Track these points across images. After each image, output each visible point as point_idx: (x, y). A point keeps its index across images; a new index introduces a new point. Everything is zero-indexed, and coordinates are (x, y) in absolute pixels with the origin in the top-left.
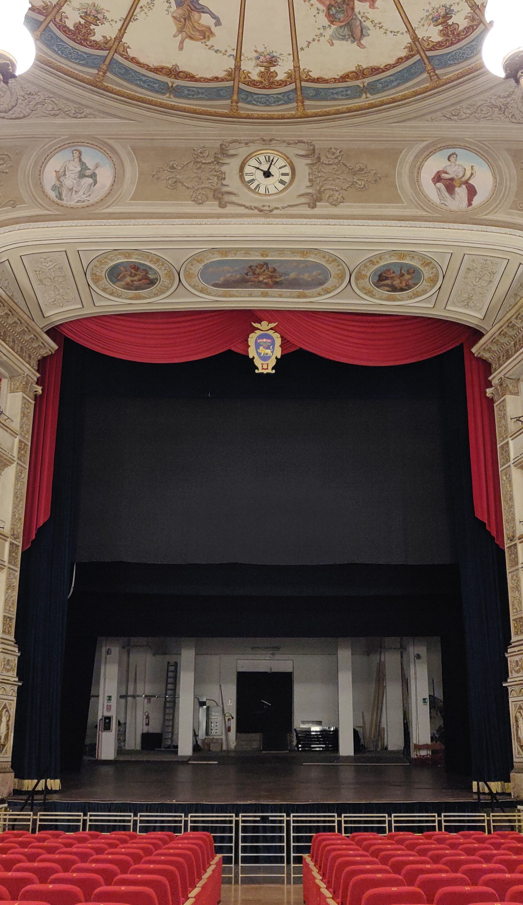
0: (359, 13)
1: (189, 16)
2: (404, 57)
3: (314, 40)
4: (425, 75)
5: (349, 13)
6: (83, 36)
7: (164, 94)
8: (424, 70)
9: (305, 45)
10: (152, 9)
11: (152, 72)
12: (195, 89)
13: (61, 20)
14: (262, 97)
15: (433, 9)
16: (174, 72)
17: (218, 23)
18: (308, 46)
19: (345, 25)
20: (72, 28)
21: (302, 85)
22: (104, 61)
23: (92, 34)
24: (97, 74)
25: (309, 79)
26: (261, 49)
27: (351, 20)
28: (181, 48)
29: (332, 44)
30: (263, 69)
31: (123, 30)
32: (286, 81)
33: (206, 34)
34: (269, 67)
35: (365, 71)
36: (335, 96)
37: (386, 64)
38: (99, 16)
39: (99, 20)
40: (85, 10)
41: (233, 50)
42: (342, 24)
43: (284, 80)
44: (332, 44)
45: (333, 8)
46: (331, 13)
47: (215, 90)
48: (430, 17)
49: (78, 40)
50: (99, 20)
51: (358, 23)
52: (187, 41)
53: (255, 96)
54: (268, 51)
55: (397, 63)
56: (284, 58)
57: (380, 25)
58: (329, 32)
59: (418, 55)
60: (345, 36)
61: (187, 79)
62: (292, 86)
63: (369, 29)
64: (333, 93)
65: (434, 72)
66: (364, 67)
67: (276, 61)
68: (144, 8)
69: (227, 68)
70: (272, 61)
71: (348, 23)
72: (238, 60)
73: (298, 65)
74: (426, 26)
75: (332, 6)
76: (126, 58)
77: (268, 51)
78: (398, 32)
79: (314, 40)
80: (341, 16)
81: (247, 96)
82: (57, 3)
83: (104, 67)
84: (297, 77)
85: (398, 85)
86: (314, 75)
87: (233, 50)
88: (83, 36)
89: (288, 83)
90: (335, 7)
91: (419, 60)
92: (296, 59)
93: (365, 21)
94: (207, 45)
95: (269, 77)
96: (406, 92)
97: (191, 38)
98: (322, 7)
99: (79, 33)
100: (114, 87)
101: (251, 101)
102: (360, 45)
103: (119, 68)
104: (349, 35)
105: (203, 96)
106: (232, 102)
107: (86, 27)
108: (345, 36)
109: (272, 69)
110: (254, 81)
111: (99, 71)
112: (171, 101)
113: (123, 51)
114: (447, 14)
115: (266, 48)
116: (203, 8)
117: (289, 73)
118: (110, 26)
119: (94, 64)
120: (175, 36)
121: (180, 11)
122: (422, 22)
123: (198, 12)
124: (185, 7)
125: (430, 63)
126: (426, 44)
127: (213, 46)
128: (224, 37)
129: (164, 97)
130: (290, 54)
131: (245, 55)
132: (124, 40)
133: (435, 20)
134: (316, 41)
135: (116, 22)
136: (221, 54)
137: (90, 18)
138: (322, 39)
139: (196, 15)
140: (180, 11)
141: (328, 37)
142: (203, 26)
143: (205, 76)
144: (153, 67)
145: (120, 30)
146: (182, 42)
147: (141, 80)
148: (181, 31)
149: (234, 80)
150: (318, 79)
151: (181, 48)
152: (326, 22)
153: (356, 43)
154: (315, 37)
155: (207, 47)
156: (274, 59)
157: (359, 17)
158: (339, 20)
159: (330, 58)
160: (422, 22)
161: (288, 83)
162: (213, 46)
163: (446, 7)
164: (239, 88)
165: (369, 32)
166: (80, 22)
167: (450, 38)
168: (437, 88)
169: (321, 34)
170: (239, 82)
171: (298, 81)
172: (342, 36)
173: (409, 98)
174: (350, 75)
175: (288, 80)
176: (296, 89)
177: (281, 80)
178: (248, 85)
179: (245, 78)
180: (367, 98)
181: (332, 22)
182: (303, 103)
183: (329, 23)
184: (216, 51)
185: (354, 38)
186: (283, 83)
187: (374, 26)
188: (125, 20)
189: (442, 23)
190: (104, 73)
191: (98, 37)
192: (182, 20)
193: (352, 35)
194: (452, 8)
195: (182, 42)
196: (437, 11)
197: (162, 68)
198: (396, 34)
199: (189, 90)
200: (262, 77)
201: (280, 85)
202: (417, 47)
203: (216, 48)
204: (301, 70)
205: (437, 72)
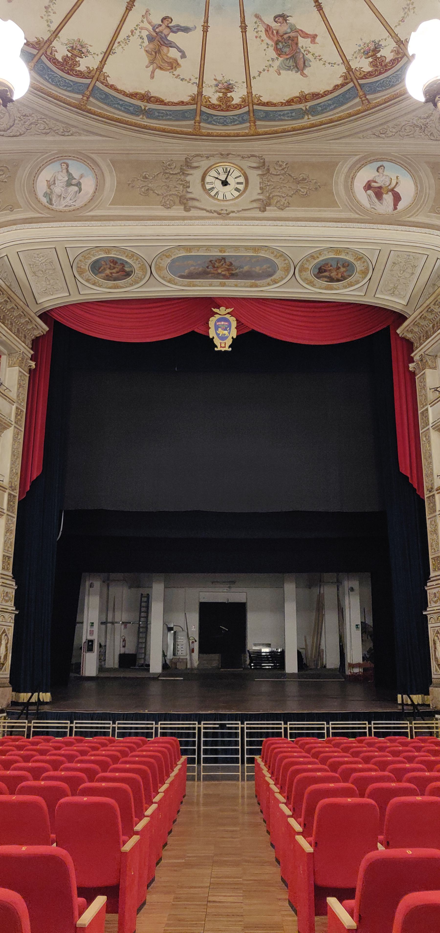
0: (302, 47)
1: (159, 50)
3: (264, 70)
4: (358, 100)
5: (294, 48)
6: (70, 67)
12: (164, 111)
13: (51, 53)
16: (146, 97)
17: (183, 56)
18: (259, 75)
19: (291, 57)
20: (60, 60)
21: (254, 108)
22: (88, 88)
23: (78, 65)
24: (82, 99)
25: (260, 103)
26: (219, 78)
28: (152, 77)
29: (279, 74)
30: (221, 95)
32: (240, 105)
33: (173, 65)
36: (282, 117)
37: (325, 90)
38: (84, 50)
39: (83, 53)
40: (72, 45)
41: (196, 78)
42: (288, 57)
45: (280, 43)
46: (279, 47)
48: (362, 51)
50: (83, 53)
51: (301, 56)
52: (158, 72)
53: (215, 118)
55: (334, 90)
57: (320, 58)
58: (277, 63)
59: (352, 83)
60: (290, 67)
61: (157, 103)
62: (246, 109)
63: (310, 61)
64: (280, 115)
65: (365, 97)
66: (306, 93)
67: (232, 88)
68: (121, 43)
69: (191, 93)
70: (229, 88)
71: (293, 56)
72: (200, 87)
74: (358, 59)
75: (280, 42)
76: (106, 86)
78: (335, 64)
79: (264, 70)
80: (287, 50)
81: (208, 117)
82: (48, 39)
83: (88, 93)
84: (250, 101)
85: (335, 108)
86: (264, 99)
87: (196, 78)
88: (70, 67)
90: (282, 43)
91: (353, 87)
92: (249, 86)
93: (307, 54)
94: (174, 75)
95: (226, 101)
96: (342, 114)
97: (161, 68)
98: (271, 43)
99: (66, 64)
100: (96, 110)
101: (211, 122)
102: (303, 74)
103: (100, 94)
106: (195, 123)
107: (72, 59)
108: (290, 67)
109: (229, 95)
111: (83, 96)
113: (104, 80)
114: (376, 48)
116: (171, 43)
119: (79, 90)
120: (147, 67)
121: (152, 46)
124: (156, 42)
125: (362, 89)
127: (179, 75)
128: (189, 68)
130: (244, 82)
131: (206, 83)
133: (366, 54)
135: (98, 55)
137: (75, 52)
139: (165, 49)
140: (152, 46)
141: (276, 68)
142: (170, 58)
143: (172, 101)
145: (101, 62)
147: (118, 104)
148: (152, 62)
149: (197, 104)
150: (267, 103)
151: (152, 77)
152: (274, 55)
153: (299, 72)
154: (265, 68)
155: (174, 76)
156: (230, 86)
157: (302, 50)
158: (286, 53)
159: (278, 85)
162: (179, 75)
164: (201, 110)
169: (270, 65)
170: (201, 105)
171: (251, 105)
173: (344, 119)
174: (295, 100)
176: (249, 111)
177: (236, 104)
178: (209, 108)
179: (206, 102)
180: (308, 119)
181: (279, 55)
183: (277, 56)
184: (182, 80)
185: (298, 68)
186: (238, 107)
187: (315, 59)
188: (105, 53)
189: (371, 56)
190: (88, 98)
191: (82, 68)
192: (153, 53)
193: (296, 66)
194: (380, 43)
195: (153, 72)
199: (159, 113)
200: (220, 101)
201: (236, 108)
202: (350, 76)
203: (181, 77)
204: (253, 96)
205: (367, 97)
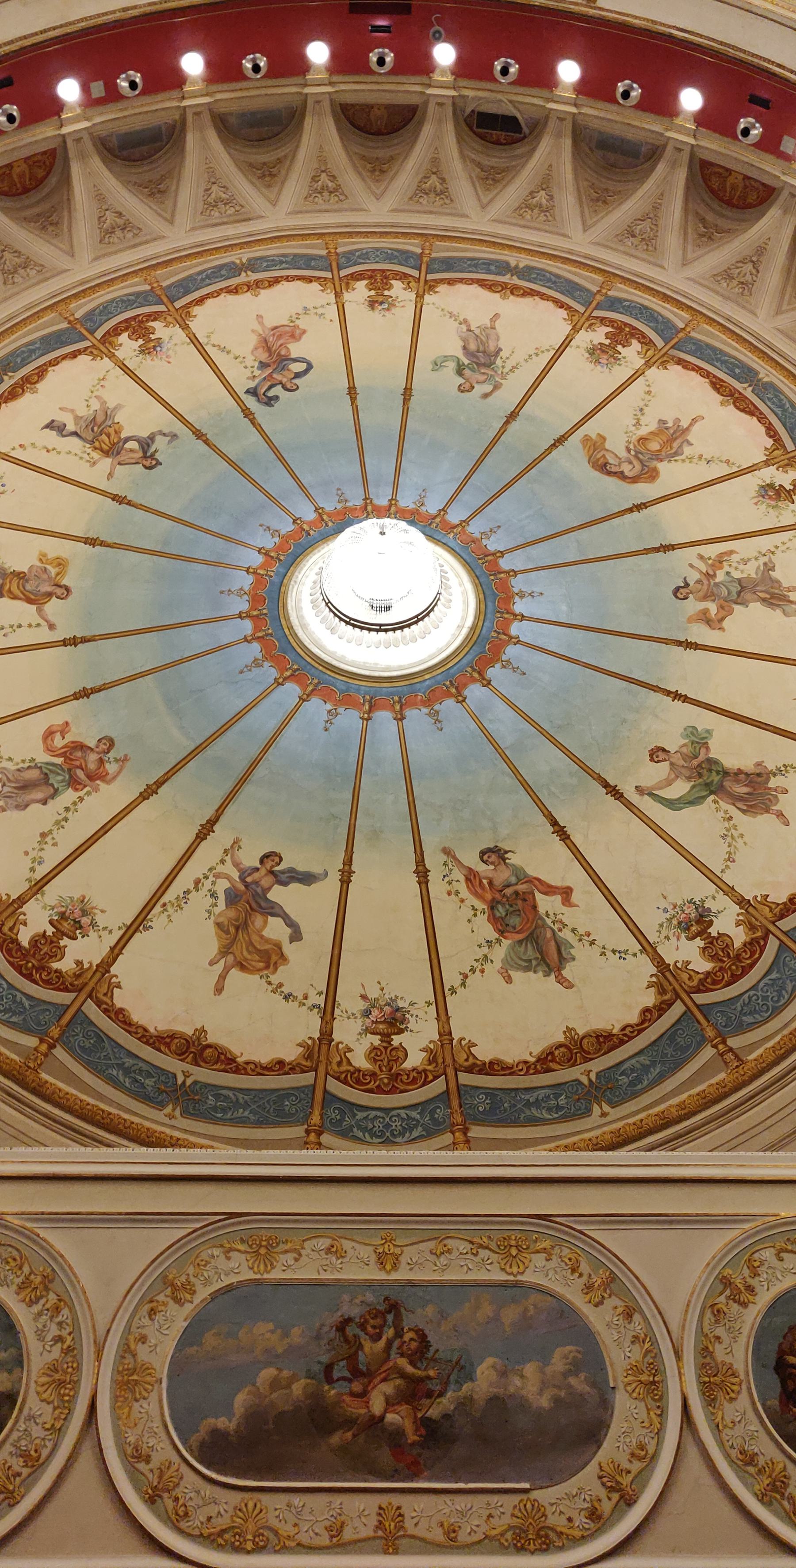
0: (547, 915)
1: (246, 923)
2: (654, 1007)
3: (473, 970)
4: (708, 1052)
5: (531, 917)
6: (39, 961)
7: (161, 1106)
8: (702, 1041)
9: (457, 983)
10: (182, 909)
11: (149, 1045)
12: (230, 1094)
13: (11, 929)
14: (376, 1117)
15: (675, 907)
16: (195, 1048)
17: (296, 936)
18: (463, 984)
19: (527, 939)
20: (25, 943)
21: (461, 1081)
22: (60, 1017)
23: (59, 957)
24: (36, 1049)
25: (474, 1065)
26: (374, 993)
27: (536, 928)
28: (219, 990)
29: (509, 980)
30: (376, 1040)
31: (116, 951)
32: (425, 1071)
33: (270, 958)
34: (388, 1035)
35: (585, 1041)
36: (535, 1112)
37: (625, 1023)
38: (85, 921)
39: (81, 927)
40: (63, 909)
41: (320, 993)
42: (520, 936)
43: (420, 1069)
44: (509, 980)
45: (500, 907)
46: (498, 915)
47: (273, 1097)
48: (675, 922)
49: (26, 969)
50: (81, 927)
51: (549, 934)
52: (235, 974)
53: (360, 1115)
54: (387, 996)
55: (643, 1022)
56: (421, 1014)
57: (591, 938)
58: (499, 953)
59: (679, 1002)
60: (530, 961)
61: (217, 1066)
62: (438, 1086)
63: (573, 947)
64: (528, 1104)
65: (724, 1042)
66: (581, 1032)
67: (404, 1020)
68: (169, 907)
69: (302, 1037)
70: (394, 1021)
71: (531, 934)
72: (328, 1017)
73: (447, 1030)
74: (673, 939)
75: (498, 902)
76: (106, 1011)
77: (387, 996)
78: (626, 952)
79: (473, 970)
80: (515, 921)
81: (342, 1113)
82: (19, 898)
83: (55, 1032)
84: (449, 1060)
85: (661, 1078)
86: (484, 1053)
87: (320, 993)
88: (39, 961)
89: (431, 1077)
90: (503, 905)
91: (685, 1013)
92: (443, 1015)
93: (560, 930)
94: (270, 983)
95: (389, 1061)
96: (684, 1096)
97: (243, 967)
98: (480, 905)
99: (34, 956)
100: (61, 1085)
101: (351, 1128)
102: (561, 980)
103: (87, 1036)
104: (537, 959)
105: (246, 1113)
106: (308, 1132)
107: (52, 942)
108: (530, 961)
109: (396, 1040)
110: (359, 1071)
111: (42, 1041)
112: (173, 1127)
113: (105, 994)
114: (701, 916)
115: (382, 989)
116: (272, 908)
117: (432, 1051)
118: (98, 940)
119: (39, 1024)
120: (211, 963)
121: (232, 913)
122: (664, 932)
123: (261, 914)
124: (242, 905)
125: (709, 1022)
126: (685, 977)
127: (280, 985)
128: (304, 967)
129: (159, 1115)
130: (429, 1004)
131: (342, 1007)
132: (113, 970)
133: (685, 926)
134: (478, 972)
135: (111, 932)
136: (296, 1004)
137: (65, 924)
138: (488, 967)
139: (258, 920)
140: (232, 913)
141: (498, 964)
142: (267, 941)
143: (257, 1060)
144: (156, 1034)
145: (112, 949)
146: (222, 977)
147: (120, 1066)
148: (225, 951)
149: (316, 1070)
150: (491, 1063)
151: (219, 990)
152: (493, 935)
153: (553, 976)
154: (475, 964)
155: (270, 988)
156: (399, 1015)
157: (549, 921)
158: (514, 928)
159: (511, 1018)
160: (664, 932)
161: (431, 1077)
162: (280, 985)
163: (695, 903)
164: (325, 1091)
165: (572, 951)
166: (45, 932)
167: (726, 965)
168: (744, 1084)
169: (486, 956)
170: (327, 1073)
171: (450, 1072)
172: (525, 961)
173: (694, 1113)
174: (557, 1053)
175: (430, 1068)
176: (447, 1092)
177: (414, 1069)
178: (345, 1082)
179: (339, 1064)
180: (604, 1115)
181: (501, 933)
182: (465, 1134)
183: (497, 936)
184: (287, 997)
185: (548, 965)
186: (420, 1077)
187: (580, 940)
188: (129, 928)
189: (698, 934)
190: (52, 1047)
191: (66, 965)
192: (232, 930)
193: (543, 959)
194: (706, 906)
195: (222, 977)
196: (683, 911)
197: (173, 1036)
198: (623, 955)
199: (217, 1096)
200: (375, 1061)
201: (414, 1081)
202: (670, 984)
203: (286, 990)
204: (454, 1042)
205: (731, 1042)
